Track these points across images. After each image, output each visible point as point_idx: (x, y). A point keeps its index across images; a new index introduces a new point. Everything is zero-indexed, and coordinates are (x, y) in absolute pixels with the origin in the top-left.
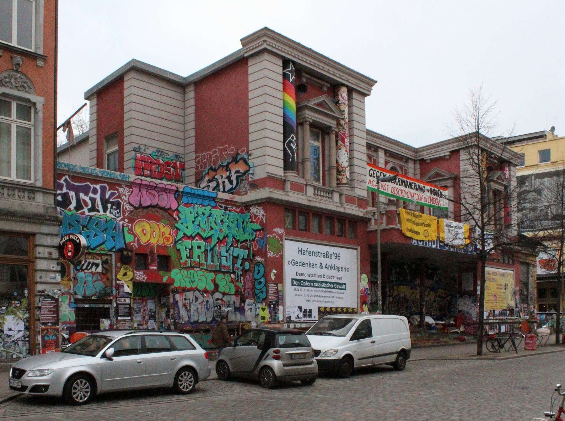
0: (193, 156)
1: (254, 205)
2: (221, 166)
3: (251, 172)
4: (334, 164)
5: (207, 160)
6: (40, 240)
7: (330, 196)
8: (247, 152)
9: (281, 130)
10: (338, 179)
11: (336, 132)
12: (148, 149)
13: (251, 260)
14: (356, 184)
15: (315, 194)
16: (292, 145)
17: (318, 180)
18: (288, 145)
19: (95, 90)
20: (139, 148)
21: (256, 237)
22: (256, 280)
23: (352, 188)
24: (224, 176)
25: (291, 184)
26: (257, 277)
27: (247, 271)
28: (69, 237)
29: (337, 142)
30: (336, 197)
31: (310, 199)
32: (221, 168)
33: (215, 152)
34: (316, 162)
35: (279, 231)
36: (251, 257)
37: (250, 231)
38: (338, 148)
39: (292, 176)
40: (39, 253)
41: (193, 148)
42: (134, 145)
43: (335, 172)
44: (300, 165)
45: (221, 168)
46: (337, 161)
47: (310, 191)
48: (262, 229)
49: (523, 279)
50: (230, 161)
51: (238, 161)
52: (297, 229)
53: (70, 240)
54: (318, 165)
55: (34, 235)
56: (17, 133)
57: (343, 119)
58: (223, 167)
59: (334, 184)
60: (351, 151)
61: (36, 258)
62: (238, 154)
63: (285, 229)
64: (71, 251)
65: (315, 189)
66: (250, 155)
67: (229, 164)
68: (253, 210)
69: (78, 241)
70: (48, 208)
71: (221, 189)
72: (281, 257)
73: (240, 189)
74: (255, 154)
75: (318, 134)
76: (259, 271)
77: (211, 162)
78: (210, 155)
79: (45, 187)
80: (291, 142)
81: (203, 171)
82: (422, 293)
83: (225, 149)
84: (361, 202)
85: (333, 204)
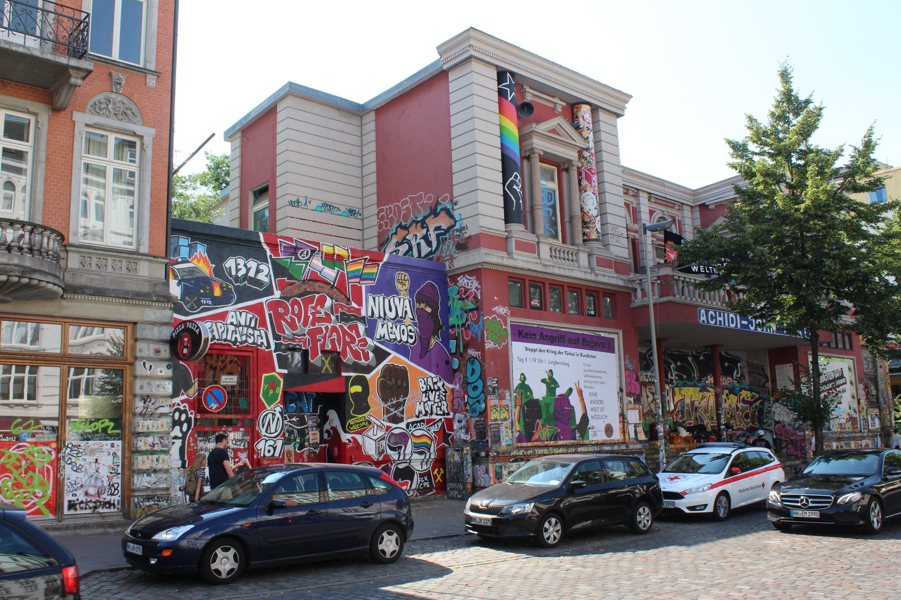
0: (374, 210)
1: (464, 274)
2: (414, 221)
3: (457, 227)
4: (578, 213)
5: (395, 214)
8: (452, 200)
9: (499, 165)
10: (584, 234)
12: (310, 202)
13: (461, 355)
14: (611, 240)
16: (515, 187)
17: (555, 237)
21: (467, 320)
22: (468, 383)
23: (606, 245)
24: (419, 236)
25: (517, 242)
26: (471, 380)
27: (455, 371)
28: (185, 325)
29: (580, 181)
31: (545, 263)
32: (414, 224)
33: (405, 203)
34: (551, 210)
35: (502, 310)
36: (462, 350)
37: (459, 312)
38: (582, 190)
39: (517, 229)
40: (141, 350)
41: (374, 199)
42: (289, 198)
43: (578, 224)
44: (528, 216)
45: (414, 224)
46: (582, 209)
47: (545, 250)
48: (477, 309)
49: (867, 368)
51: (439, 213)
52: (528, 306)
53: (187, 330)
54: (555, 214)
55: (135, 323)
58: (417, 222)
59: (579, 239)
62: (437, 203)
66: (456, 204)
67: (425, 218)
68: (463, 281)
69: (197, 331)
70: (155, 285)
73: (442, 252)
74: (462, 201)
75: (553, 171)
76: (473, 370)
78: (398, 206)
79: (154, 254)
80: (513, 182)
81: (389, 230)
82: (717, 396)
83: (420, 198)
84: (618, 266)
85: (579, 269)
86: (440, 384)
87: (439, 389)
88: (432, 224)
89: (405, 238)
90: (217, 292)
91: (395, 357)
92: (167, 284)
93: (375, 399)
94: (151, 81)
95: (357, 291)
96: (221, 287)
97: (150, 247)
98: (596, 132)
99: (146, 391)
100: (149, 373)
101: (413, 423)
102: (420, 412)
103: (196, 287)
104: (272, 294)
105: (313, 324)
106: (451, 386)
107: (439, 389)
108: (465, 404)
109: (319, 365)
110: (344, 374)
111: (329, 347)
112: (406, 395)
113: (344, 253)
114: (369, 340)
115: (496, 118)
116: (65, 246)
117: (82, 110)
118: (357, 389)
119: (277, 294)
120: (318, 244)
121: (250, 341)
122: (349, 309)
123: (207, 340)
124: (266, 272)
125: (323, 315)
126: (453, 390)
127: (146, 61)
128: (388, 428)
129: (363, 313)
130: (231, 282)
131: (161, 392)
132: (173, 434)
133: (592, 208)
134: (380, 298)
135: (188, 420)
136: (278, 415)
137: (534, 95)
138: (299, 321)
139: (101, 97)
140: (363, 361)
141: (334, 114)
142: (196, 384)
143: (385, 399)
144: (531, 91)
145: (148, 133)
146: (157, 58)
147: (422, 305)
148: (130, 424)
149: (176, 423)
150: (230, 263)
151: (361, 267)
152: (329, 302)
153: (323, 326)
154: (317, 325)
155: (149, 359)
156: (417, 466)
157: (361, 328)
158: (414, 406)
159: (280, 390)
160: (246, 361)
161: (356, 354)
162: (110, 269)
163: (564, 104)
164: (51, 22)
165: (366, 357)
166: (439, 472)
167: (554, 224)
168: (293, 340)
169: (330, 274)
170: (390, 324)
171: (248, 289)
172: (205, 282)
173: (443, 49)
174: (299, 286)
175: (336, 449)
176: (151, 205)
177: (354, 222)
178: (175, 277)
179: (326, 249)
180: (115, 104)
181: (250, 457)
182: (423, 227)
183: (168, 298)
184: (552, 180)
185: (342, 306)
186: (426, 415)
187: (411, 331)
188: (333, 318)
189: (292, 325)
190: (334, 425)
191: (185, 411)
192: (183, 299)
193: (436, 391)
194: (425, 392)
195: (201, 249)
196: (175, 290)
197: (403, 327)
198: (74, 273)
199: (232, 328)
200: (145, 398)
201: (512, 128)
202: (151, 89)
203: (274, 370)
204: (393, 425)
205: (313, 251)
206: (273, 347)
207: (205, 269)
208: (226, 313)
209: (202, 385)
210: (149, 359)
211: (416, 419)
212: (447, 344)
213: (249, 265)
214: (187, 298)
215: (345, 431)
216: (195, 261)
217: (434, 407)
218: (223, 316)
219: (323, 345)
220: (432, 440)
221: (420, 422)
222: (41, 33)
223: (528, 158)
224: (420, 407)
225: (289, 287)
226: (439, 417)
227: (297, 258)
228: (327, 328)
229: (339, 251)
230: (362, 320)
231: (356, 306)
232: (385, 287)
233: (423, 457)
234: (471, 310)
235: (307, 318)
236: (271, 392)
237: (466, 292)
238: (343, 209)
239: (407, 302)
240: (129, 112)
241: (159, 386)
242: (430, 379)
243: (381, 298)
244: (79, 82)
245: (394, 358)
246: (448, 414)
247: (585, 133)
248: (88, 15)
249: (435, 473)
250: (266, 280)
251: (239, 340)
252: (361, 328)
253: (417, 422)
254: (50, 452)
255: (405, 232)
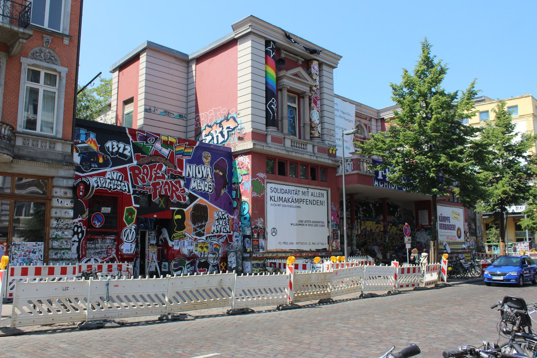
3: (239, 127)
4: (307, 121)
5: (205, 118)
6: (56, 182)
7: (305, 147)
10: (311, 134)
11: (309, 97)
14: (325, 137)
15: (291, 146)
16: (272, 106)
17: (295, 135)
18: (270, 106)
19: (117, 65)
20: (150, 109)
27: (235, 208)
28: (82, 179)
30: (310, 148)
33: (211, 112)
38: (311, 109)
40: (56, 193)
43: (308, 128)
44: (280, 123)
45: (215, 125)
46: (310, 120)
47: (288, 143)
50: (222, 119)
54: (294, 122)
55: (53, 177)
56: (44, 95)
57: (316, 86)
58: (217, 124)
59: (308, 137)
60: (321, 111)
61: (53, 197)
63: (267, 173)
64: (82, 191)
65: (292, 142)
66: (239, 114)
67: (222, 122)
69: (88, 183)
70: (65, 156)
71: (216, 142)
72: (264, 196)
74: (242, 113)
75: (295, 98)
77: (207, 120)
80: (272, 104)
85: (308, 153)
86: (226, 216)
87: (225, 218)
88: (225, 125)
89: (210, 133)
90: (101, 161)
91: (201, 199)
92: (72, 155)
93: (188, 222)
94: (66, 41)
95: (180, 162)
96: (103, 158)
97: (63, 134)
98: (320, 76)
99: (58, 215)
100: (60, 205)
101: (209, 237)
102: (214, 231)
103: (89, 158)
104: (132, 162)
105: (155, 180)
106: (232, 217)
107: (225, 218)
108: (240, 227)
109: (158, 203)
110: (171, 208)
111: (163, 193)
112: (206, 221)
113: (174, 140)
114: (186, 190)
115: (263, 67)
116: (14, 133)
117: (26, 56)
118: (179, 217)
119: (135, 163)
120: (159, 135)
121: (119, 188)
122: (176, 172)
123: (93, 187)
124: (129, 150)
125: (160, 175)
126: (233, 219)
127: (64, 30)
128: (196, 239)
129: (184, 175)
130: (109, 155)
131: (67, 216)
132: (73, 239)
133: (316, 119)
134: (193, 166)
135: (82, 232)
136: (133, 230)
137: (286, 54)
138: (147, 178)
139: (37, 49)
140: (182, 201)
141: (174, 61)
142: (87, 212)
143: (194, 223)
144: (285, 52)
145: (64, 70)
146: (70, 28)
147: (218, 171)
148: (49, 233)
149: (76, 233)
150: (109, 144)
151: (183, 148)
152: (164, 168)
153: (160, 181)
154: (157, 181)
155: (61, 197)
156: (211, 262)
157: (182, 183)
158: (211, 227)
159: (135, 216)
160: (116, 199)
161: (178, 197)
162: (39, 146)
163: (303, 60)
164: (9, 6)
165: (184, 199)
166: (223, 265)
167: (294, 128)
168: (143, 188)
169: (165, 152)
170: (199, 181)
171: (119, 159)
172: (94, 154)
173: (235, 27)
174: (148, 159)
175: (166, 250)
176: (64, 111)
177: (182, 122)
178: (77, 151)
179: (164, 138)
180: (45, 53)
181: (117, 253)
182: (220, 127)
183: (72, 164)
184: (295, 102)
185: (172, 170)
186: (217, 232)
187: (210, 185)
188: (166, 177)
189: (143, 180)
190: (164, 237)
191: (81, 227)
192: (81, 163)
193: (223, 219)
194: (217, 220)
195: (93, 136)
196: (77, 159)
197: (206, 183)
198: (19, 148)
199: (108, 181)
200: (58, 219)
201: (272, 73)
202: (67, 45)
203: (132, 205)
204: (199, 238)
205: (156, 139)
206: (132, 192)
207: (94, 147)
208: (106, 172)
209: (90, 212)
210: (61, 197)
211: (211, 235)
212: (231, 194)
213: (119, 146)
214: (84, 163)
215: (171, 240)
216: (89, 143)
217: (222, 228)
218: (104, 174)
219: (160, 192)
220: (220, 247)
221: (213, 236)
222: (3, 13)
223: (281, 90)
224: (214, 228)
225: (142, 159)
226: (225, 234)
227: (147, 143)
228: (162, 182)
229: (170, 139)
230: (183, 178)
231: (180, 171)
232: (197, 160)
233: (215, 256)
234: (244, 175)
235: (151, 176)
236: (130, 217)
237: (242, 165)
238: (176, 114)
239: (209, 169)
240: (53, 58)
241: (65, 212)
242: (220, 213)
243: (194, 166)
244: (25, 41)
245: (200, 200)
246: (230, 232)
247: (315, 77)
248: (31, 3)
249: (221, 265)
250: (129, 154)
251: (113, 188)
252: (182, 183)
253: (212, 236)
254: (3, 248)
255: (210, 129)
